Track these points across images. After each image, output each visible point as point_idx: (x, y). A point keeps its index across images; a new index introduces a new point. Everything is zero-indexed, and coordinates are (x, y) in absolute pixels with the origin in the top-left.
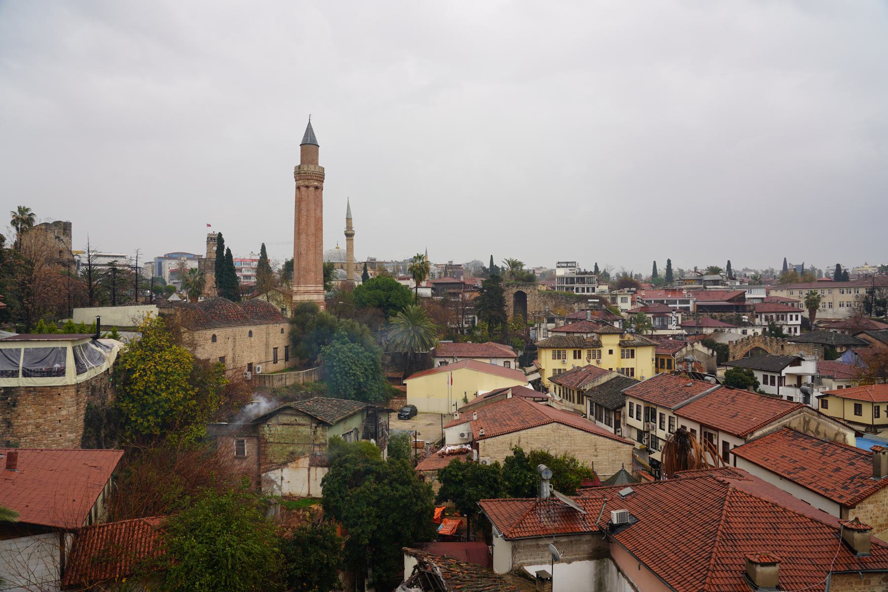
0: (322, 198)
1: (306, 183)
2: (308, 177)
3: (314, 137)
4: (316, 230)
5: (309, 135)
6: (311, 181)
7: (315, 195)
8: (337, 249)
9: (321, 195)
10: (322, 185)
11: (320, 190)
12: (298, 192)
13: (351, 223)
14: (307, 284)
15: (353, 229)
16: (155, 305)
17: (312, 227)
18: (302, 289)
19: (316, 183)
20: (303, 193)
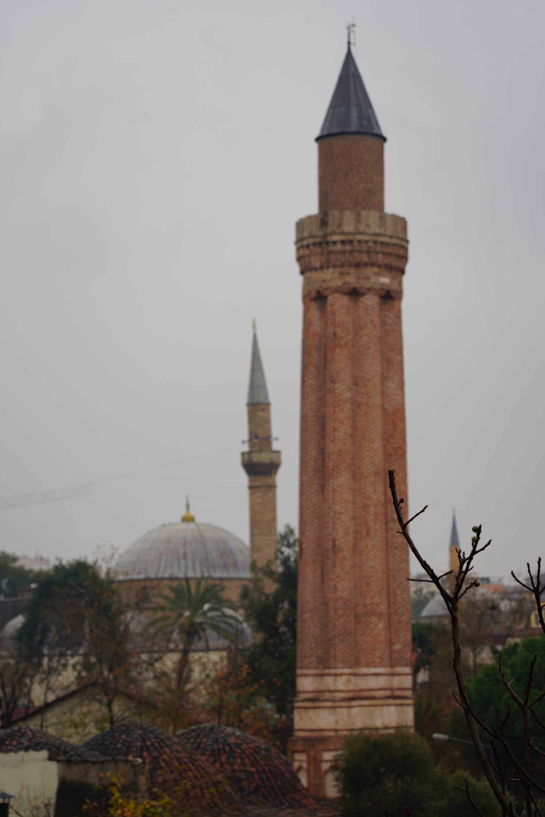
0: (400, 332)
1: (352, 280)
2: (357, 257)
3: (369, 106)
4: (387, 456)
5: (353, 101)
6: (370, 271)
7: (383, 323)
8: (184, 526)
9: (398, 317)
10: (400, 284)
11: (395, 303)
12: (315, 314)
13: (268, 421)
14: (357, 663)
15: (275, 446)
16: (44, 754)
17: (377, 445)
18: (341, 684)
19: (385, 280)
20: (341, 317)
